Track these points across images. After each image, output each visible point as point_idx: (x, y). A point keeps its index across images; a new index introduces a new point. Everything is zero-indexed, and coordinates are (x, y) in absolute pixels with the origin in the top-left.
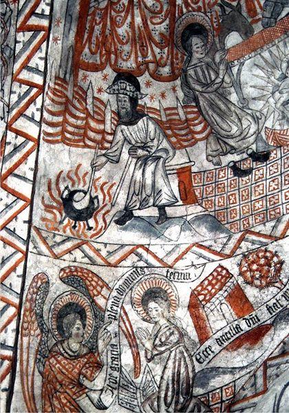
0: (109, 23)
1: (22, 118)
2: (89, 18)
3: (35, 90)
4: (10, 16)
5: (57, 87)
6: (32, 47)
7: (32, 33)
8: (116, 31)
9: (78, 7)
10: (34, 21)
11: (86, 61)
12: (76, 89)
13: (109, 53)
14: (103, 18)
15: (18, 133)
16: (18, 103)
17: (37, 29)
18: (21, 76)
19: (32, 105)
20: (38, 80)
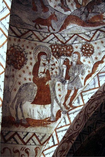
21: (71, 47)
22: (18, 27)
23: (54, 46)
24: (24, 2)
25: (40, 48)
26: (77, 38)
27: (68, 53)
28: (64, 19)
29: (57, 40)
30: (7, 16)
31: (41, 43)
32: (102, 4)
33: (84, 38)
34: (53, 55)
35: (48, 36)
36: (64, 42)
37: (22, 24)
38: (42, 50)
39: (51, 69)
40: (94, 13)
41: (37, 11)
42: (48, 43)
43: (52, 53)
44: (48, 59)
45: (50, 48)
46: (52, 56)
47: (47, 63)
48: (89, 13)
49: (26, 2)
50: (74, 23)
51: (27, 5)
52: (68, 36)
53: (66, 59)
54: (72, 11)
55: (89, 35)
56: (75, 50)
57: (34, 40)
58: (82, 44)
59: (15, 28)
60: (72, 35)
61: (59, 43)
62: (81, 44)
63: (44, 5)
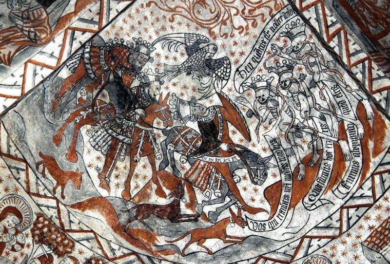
0: (369, 6)
1: (374, 82)
2: (356, 12)
3: (367, 62)
4: (315, 47)
5: (375, 57)
6: (343, 43)
7: (336, 37)
8: (377, 7)
9: (345, 11)
10: (332, 30)
11: (377, 33)
12: (386, 51)
13: (384, 20)
14: (363, 5)
15: (379, 91)
16: (364, 76)
17: (337, 33)
18: (352, 62)
19: (373, 70)
20: (363, 55)
21: (71, 244)
22: (11, 138)
23: (45, 219)
24: (50, 116)
25: (19, 201)
26: (92, 239)
27: (61, 249)
28: (90, 196)
29: (56, 215)
30: (11, 97)
31: (26, 196)
32: (166, 221)
33: (105, 249)
34: (33, 231)
35: (45, 196)
36: (66, 228)
37: (22, 137)
38: (19, 206)
39: (11, 248)
40: (144, 224)
41: (57, 145)
42: (38, 205)
43: (32, 226)
44: (19, 228)
45: (35, 217)
46: (29, 231)
47: (13, 232)
48: (136, 218)
49: (51, 118)
50: (103, 215)
51: (51, 123)
52: (79, 224)
53: (50, 254)
54: (112, 194)
55: (115, 250)
56: (75, 254)
57: (19, 181)
58: (94, 254)
59: (6, 134)
60: (86, 229)
61: (57, 222)
62: (93, 253)
63: (74, 148)
